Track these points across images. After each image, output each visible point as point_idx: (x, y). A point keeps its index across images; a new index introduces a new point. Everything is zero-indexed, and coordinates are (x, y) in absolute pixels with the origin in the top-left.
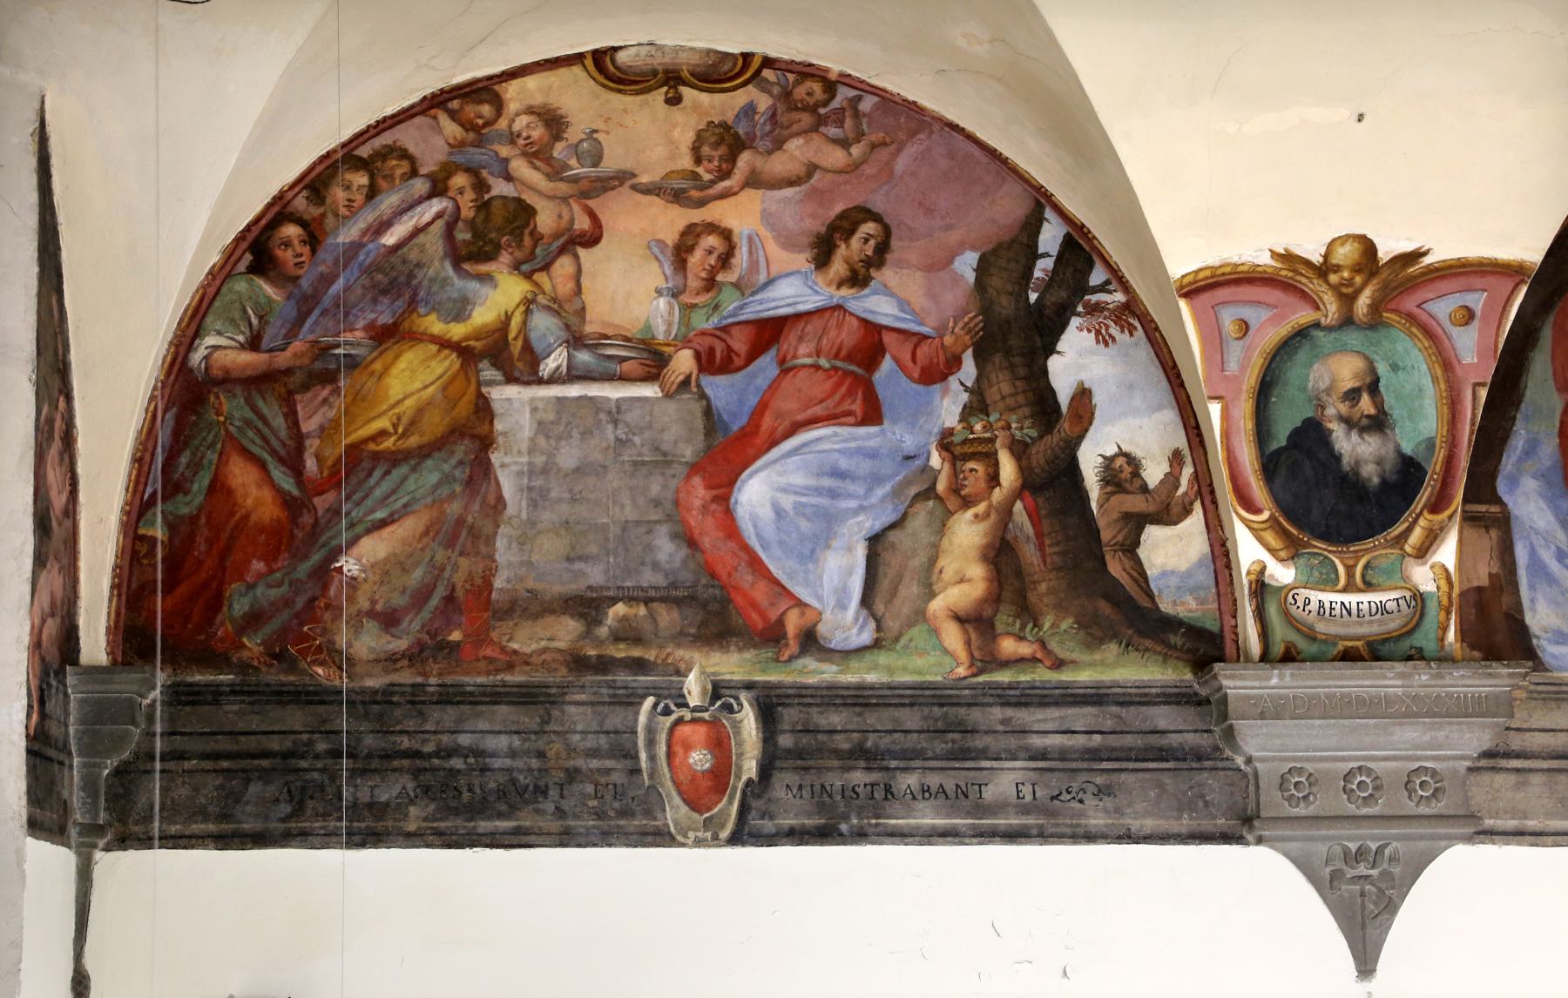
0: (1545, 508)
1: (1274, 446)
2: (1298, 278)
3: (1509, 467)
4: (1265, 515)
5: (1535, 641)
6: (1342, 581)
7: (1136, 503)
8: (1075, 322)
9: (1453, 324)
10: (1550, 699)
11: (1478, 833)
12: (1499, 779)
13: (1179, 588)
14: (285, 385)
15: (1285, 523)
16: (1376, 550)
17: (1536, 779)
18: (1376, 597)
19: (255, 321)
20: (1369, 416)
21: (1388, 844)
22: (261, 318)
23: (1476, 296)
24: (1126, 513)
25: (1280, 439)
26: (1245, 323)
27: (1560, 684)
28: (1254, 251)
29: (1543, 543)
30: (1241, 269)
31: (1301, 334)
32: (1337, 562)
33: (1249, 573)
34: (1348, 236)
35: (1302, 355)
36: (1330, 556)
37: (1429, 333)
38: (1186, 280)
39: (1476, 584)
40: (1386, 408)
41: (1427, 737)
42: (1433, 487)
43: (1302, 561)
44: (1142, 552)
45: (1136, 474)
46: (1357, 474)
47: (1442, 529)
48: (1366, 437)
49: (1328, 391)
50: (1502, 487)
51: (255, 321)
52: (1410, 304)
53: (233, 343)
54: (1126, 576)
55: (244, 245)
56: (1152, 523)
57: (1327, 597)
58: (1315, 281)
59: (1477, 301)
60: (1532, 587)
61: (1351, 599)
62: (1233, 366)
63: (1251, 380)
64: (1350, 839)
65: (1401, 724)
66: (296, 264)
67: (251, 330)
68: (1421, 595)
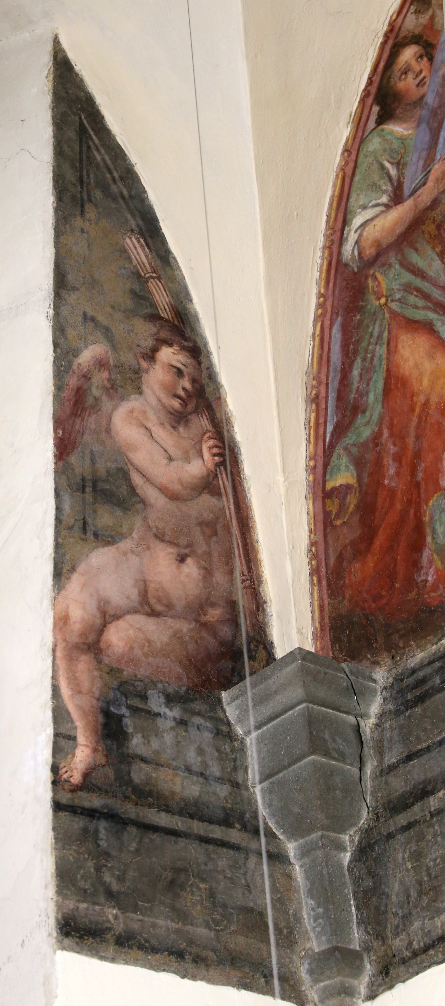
14: (434, 221)
19: (393, 172)
22: (398, 165)
51: (393, 172)
53: (378, 209)
55: (370, 100)
66: (418, 85)
67: (392, 184)
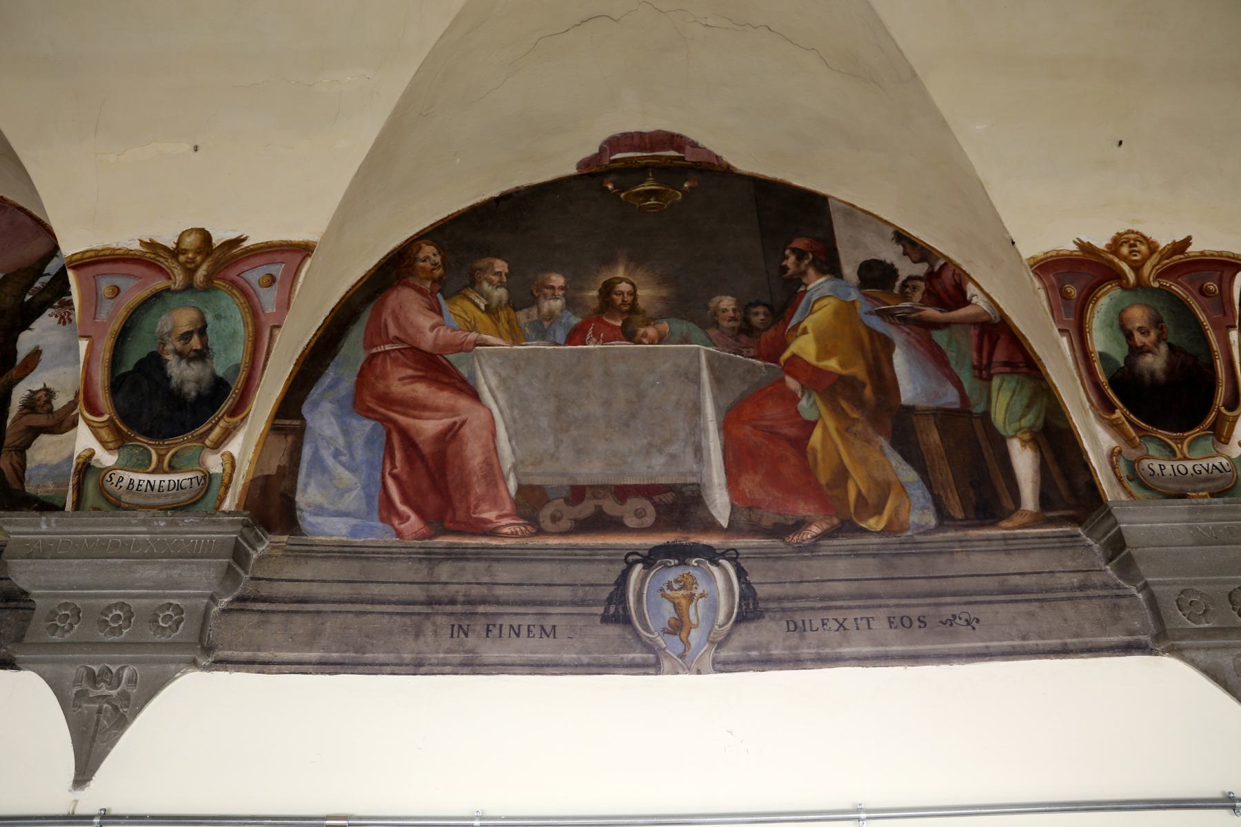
0: (334, 422)
1: (123, 370)
2: (158, 258)
3: (315, 395)
4: (106, 417)
5: (298, 513)
6: (153, 465)
7: (39, 420)
8: (49, 311)
9: (261, 286)
10: (301, 556)
11: (215, 662)
12: (244, 618)
13: (45, 476)
15: (119, 424)
16: (183, 443)
17: (276, 618)
18: (175, 477)
20: (195, 350)
21: (124, 667)
23: (277, 266)
24: (30, 426)
25: (130, 364)
26: (118, 288)
27: (312, 545)
28: (128, 239)
29: (325, 444)
30: (117, 252)
31: (157, 296)
32: (153, 452)
33: (78, 457)
34: (192, 230)
35: (155, 310)
36: (149, 447)
37: (244, 293)
38: (74, 258)
39: (266, 473)
40: (209, 345)
41: (164, 575)
42: (234, 399)
43: (126, 450)
44: (29, 453)
45: (48, 402)
46: (180, 390)
47: (235, 428)
48: (192, 364)
49: (169, 334)
50: (305, 409)
52: (233, 274)
54: (10, 467)
56: (45, 433)
57: (137, 477)
58: (169, 261)
59: (277, 270)
60: (308, 476)
61: (156, 479)
62: (103, 316)
63: (116, 325)
64: (92, 663)
65: (143, 564)
68: (210, 475)
